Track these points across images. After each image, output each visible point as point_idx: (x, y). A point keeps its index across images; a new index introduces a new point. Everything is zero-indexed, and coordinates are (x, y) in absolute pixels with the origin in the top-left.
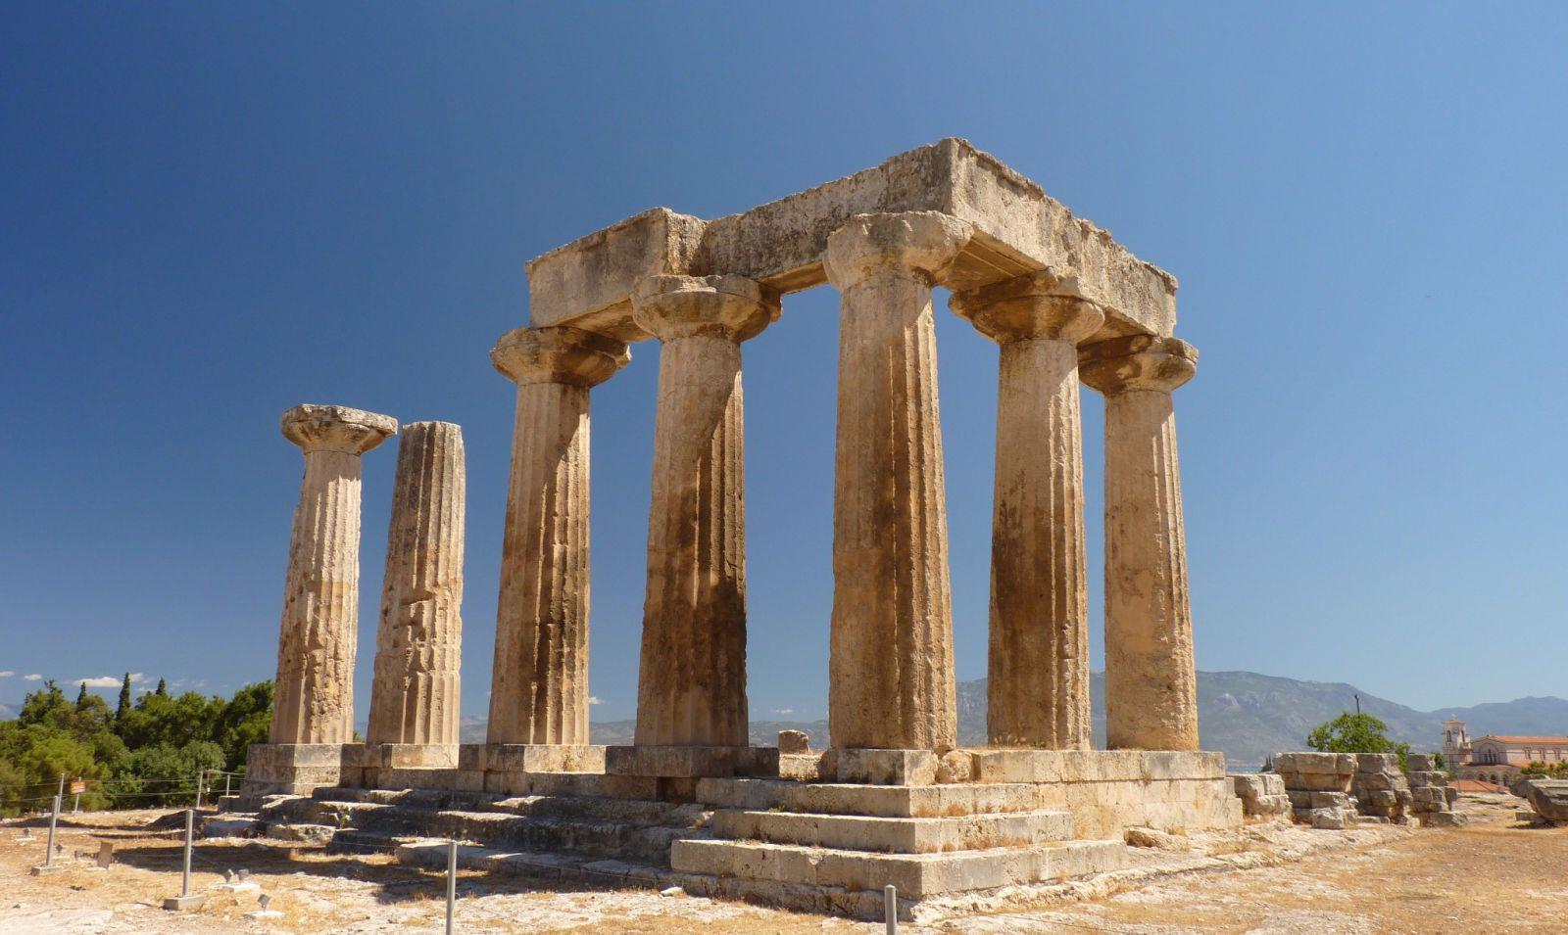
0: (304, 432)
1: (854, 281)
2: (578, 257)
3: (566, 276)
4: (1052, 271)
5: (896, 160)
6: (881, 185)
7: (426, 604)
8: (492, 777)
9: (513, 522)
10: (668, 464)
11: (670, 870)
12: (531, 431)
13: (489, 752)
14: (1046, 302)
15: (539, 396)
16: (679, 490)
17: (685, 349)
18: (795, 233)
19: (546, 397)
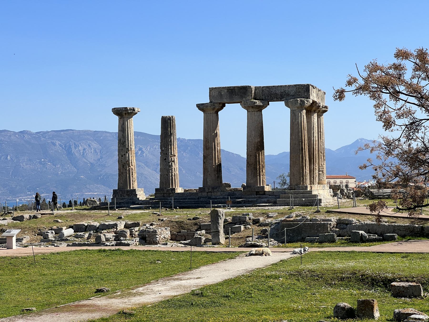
0: (126, 114)
1: (295, 109)
2: (226, 91)
3: (222, 93)
4: (317, 102)
5: (298, 85)
6: (295, 89)
7: (175, 157)
8: (209, 193)
9: (208, 143)
10: (253, 136)
11: (276, 203)
12: (211, 124)
13: (209, 189)
14: (315, 107)
15: (213, 116)
16: (256, 141)
17: (256, 114)
18: (276, 93)
19: (214, 117)
